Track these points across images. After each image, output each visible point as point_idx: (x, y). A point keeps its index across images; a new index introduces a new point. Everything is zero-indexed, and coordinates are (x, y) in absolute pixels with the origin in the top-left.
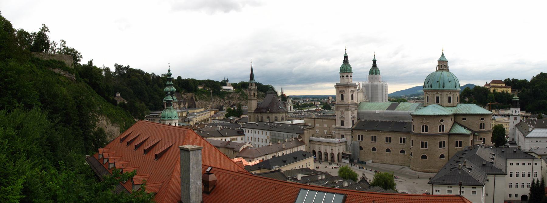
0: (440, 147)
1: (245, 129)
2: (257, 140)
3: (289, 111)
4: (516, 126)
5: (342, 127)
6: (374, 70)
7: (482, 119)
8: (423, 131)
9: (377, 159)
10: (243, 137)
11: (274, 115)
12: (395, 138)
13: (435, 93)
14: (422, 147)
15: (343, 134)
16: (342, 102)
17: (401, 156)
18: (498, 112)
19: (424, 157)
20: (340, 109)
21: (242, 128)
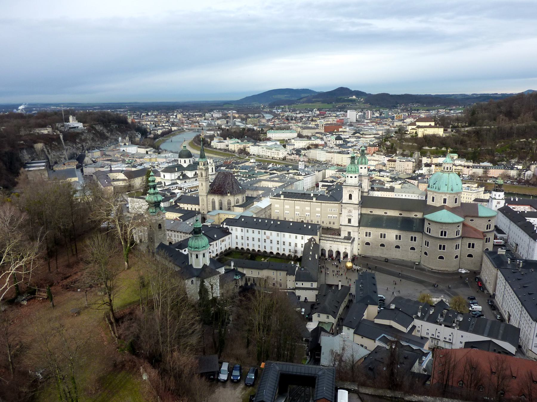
0: (456, 249)
1: (231, 227)
2: (251, 239)
3: (210, 174)
4: (499, 210)
5: (349, 224)
6: (364, 159)
7: (490, 221)
8: (442, 235)
9: (385, 254)
10: (230, 235)
11: (236, 198)
12: (406, 236)
13: (443, 195)
14: (440, 249)
15: (349, 231)
16: (350, 201)
17: (411, 252)
18: (430, 160)
19: (441, 258)
20: (347, 208)
21: (226, 226)
